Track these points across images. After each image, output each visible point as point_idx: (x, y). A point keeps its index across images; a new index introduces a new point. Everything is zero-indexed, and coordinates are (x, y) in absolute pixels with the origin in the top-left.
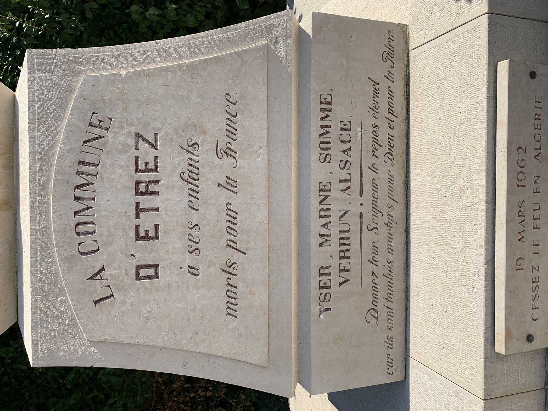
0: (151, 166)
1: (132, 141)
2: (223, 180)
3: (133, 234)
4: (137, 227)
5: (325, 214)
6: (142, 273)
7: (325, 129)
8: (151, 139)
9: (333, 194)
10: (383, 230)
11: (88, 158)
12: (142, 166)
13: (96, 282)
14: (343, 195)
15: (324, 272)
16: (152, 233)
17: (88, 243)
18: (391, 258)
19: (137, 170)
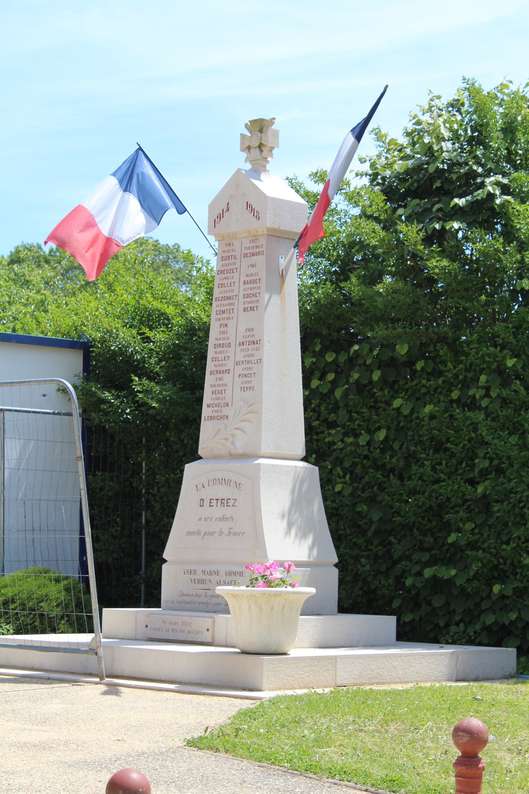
0: (228, 504)
1: (235, 498)
2: (222, 531)
3: (212, 498)
4: (213, 499)
5: (211, 573)
6: (202, 501)
7: (235, 573)
8: (235, 504)
9: (216, 576)
10: (204, 600)
11: (232, 482)
12: (228, 501)
13: (201, 486)
14: (216, 582)
15: (195, 572)
16: (211, 504)
17: (211, 483)
18: (197, 603)
19: (228, 499)
